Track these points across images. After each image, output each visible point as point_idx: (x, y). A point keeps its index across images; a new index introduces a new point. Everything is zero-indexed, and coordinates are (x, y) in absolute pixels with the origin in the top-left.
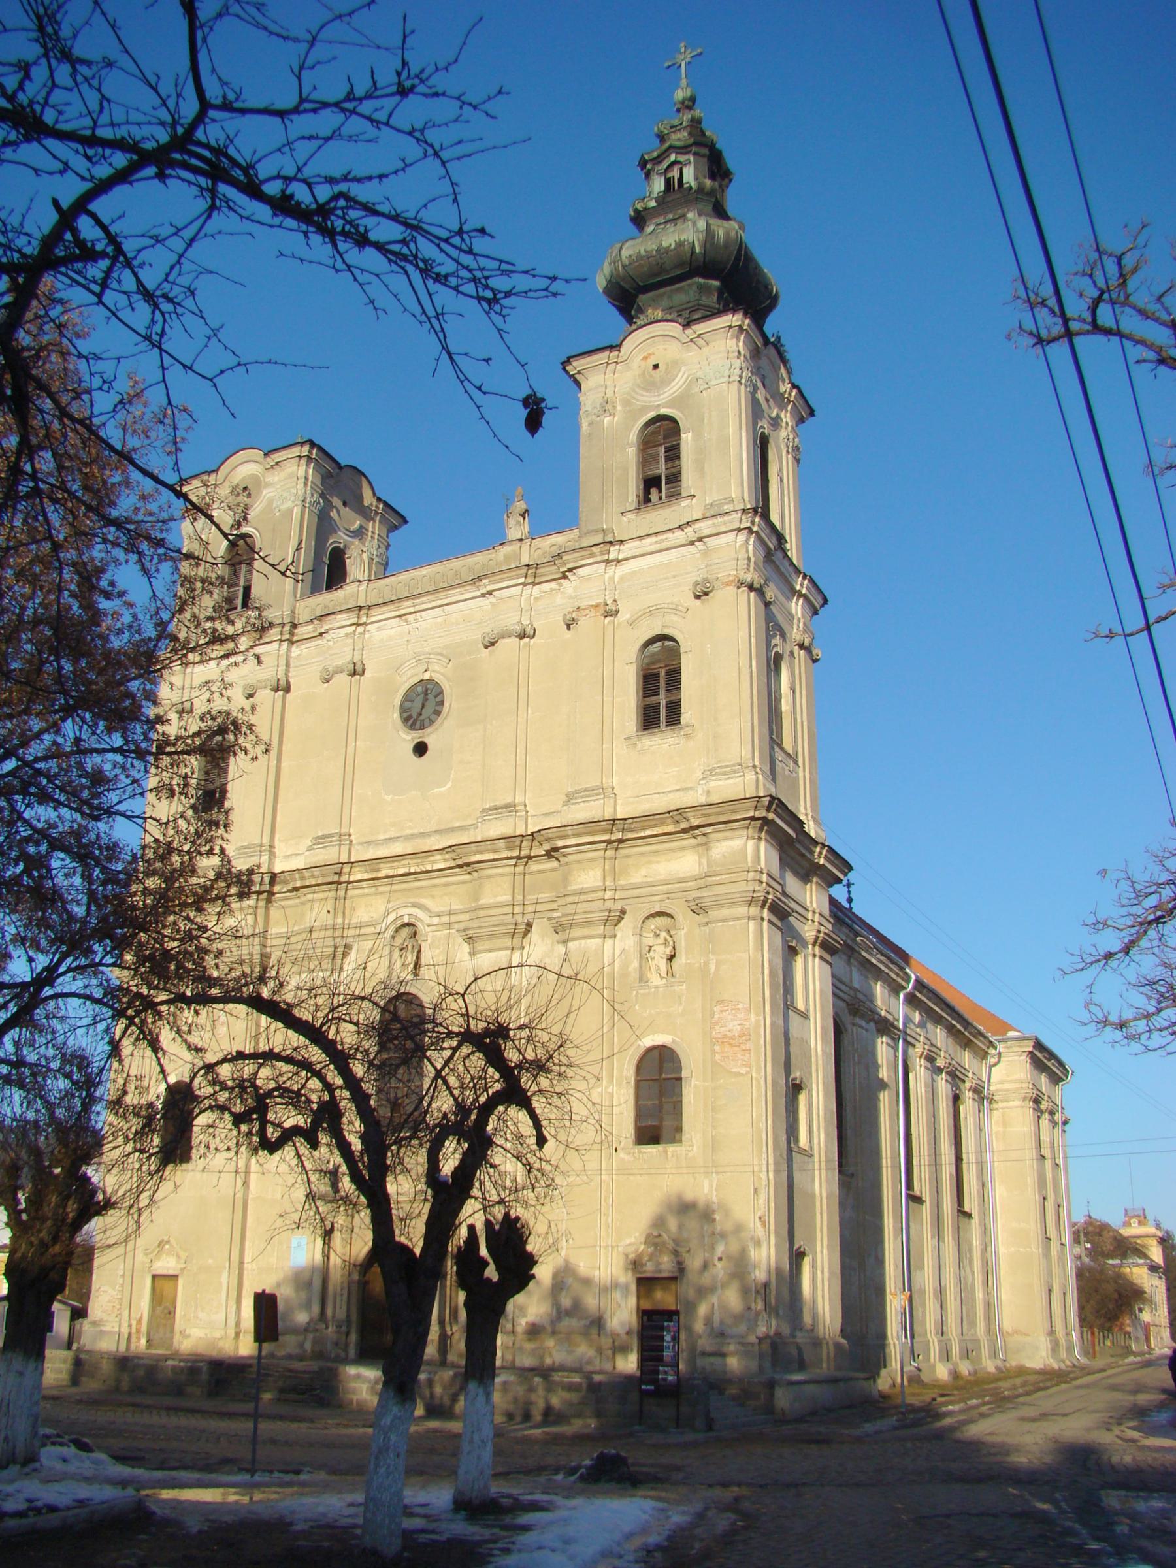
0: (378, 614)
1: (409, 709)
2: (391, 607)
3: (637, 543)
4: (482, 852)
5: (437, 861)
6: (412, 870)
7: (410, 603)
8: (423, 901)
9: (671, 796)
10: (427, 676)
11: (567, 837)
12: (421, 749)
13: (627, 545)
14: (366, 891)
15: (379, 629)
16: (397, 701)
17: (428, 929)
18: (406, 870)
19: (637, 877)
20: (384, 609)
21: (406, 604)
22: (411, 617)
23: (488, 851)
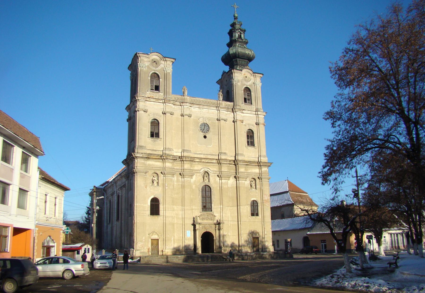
0: (195, 106)
1: (201, 128)
2: (198, 105)
3: (247, 111)
4: (224, 161)
5: (214, 161)
6: (209, 162)
7: (202, 106)
8: (209, 168)
9: (254, 158)
10: (205, 122)
11: (241, 162)
12: (205, 137)
13: (246, 111)
14: (197, 163)
15: (194, 109)
16: (199, 125)
17: (211, 173)
18: (207, 161)
19: (249, 171)
20: (197, 105)
21: (201, 106)
22: (201, 109)
23: (225, 161)
